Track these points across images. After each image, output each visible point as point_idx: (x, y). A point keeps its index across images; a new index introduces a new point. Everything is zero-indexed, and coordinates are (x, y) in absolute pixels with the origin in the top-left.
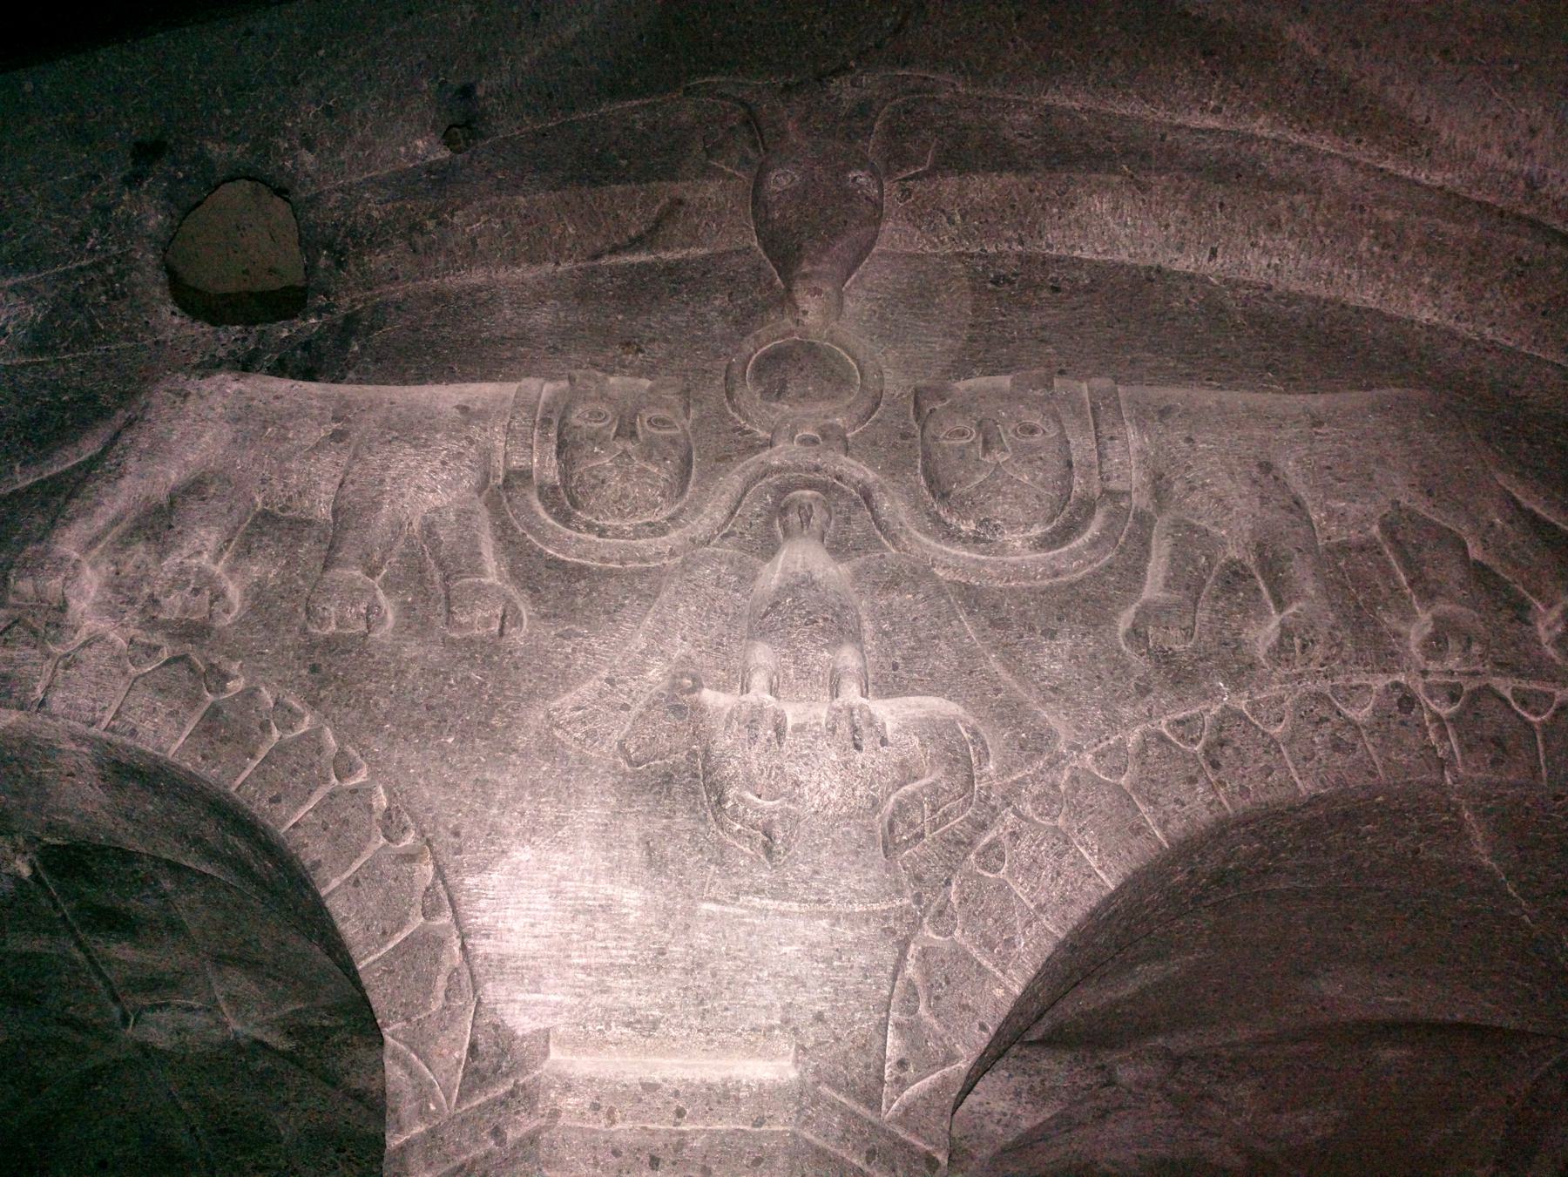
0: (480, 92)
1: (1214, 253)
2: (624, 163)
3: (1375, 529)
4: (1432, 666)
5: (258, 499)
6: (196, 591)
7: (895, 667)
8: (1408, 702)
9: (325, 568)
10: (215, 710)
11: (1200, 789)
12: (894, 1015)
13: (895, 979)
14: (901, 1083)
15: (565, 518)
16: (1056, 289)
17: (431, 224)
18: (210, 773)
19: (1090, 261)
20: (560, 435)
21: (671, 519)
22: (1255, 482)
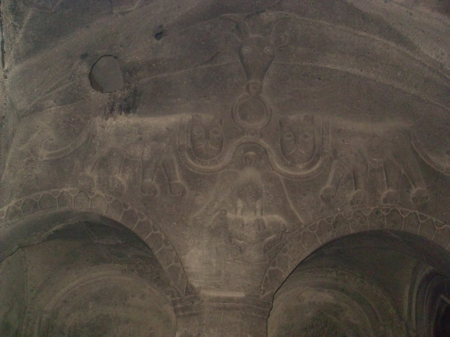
0: (165, 26)
1: (362, 70)
2: (203, 43)
3: (382, 165)
4: (384, 205)
5: (124, 155)
6: (118, 185)
7: (269, 204)
8: (377, 212)
9: (143, 179)
10: (126, 213)
11: (330, 233)
12: (263, 283)
13: (263, 277)
14: (264, 294)
15: (193, 159)
16: (320, 79)
17: (154, 65)
18: (128, 227)
19: (330, 68)
20: (191, 136)
21: (219, 159)
22: (356, 155)
